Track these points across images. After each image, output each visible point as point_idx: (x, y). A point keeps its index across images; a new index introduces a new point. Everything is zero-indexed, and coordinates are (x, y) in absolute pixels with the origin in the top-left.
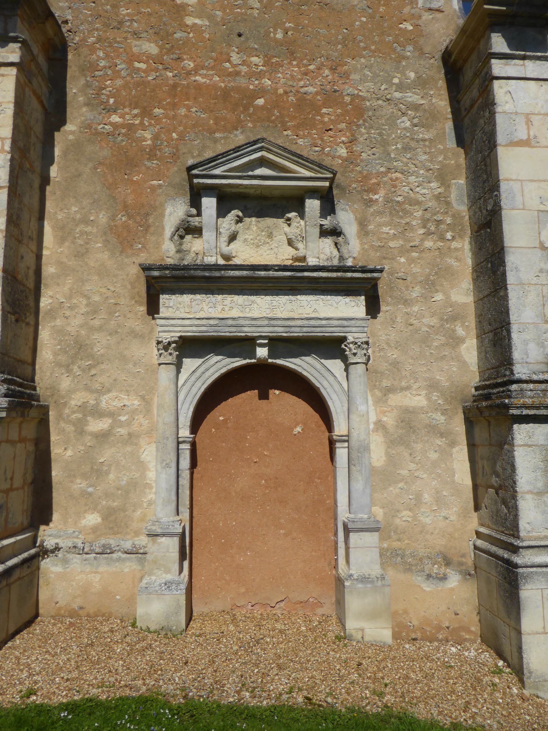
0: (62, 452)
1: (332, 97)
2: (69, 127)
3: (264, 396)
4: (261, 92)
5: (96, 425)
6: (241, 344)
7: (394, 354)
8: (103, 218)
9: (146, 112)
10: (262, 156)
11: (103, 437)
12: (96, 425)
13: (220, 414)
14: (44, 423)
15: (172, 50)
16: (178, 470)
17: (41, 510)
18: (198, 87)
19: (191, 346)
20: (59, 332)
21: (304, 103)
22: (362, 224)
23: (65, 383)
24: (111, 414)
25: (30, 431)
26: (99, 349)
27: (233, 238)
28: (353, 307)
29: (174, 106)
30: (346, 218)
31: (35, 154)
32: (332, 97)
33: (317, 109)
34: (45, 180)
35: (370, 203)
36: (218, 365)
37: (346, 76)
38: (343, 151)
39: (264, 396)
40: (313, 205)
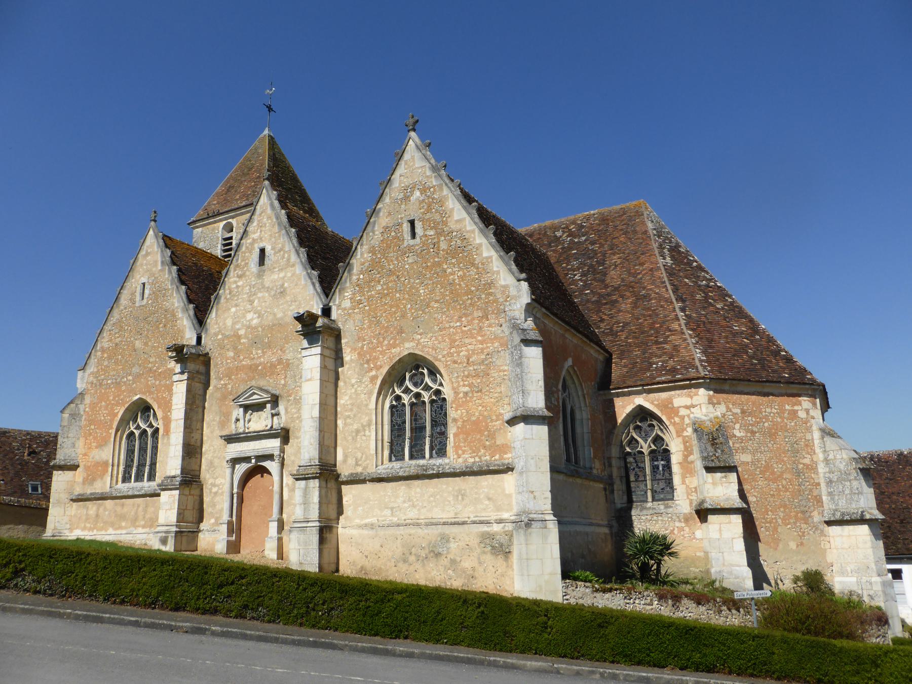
0: (206, 499)
1: (280, 361)
2: (211, 388)
3: (262, 476)
4: (260, 364)
5: (215, 490)
6: (247, 459)
7: (293, 458)
8: (217, 419)
9: (230, 379)
10: (140, 399)
11: (216, 493)
12: (215, 490)
13: (250, 484)
14: (202, 489)
15: (237, 352)
16: (455, 524)
17: (201, 519)
18: (244, 366)
19: (235, 461)
20: (206, 459)
21: (273, 366)
22: (286, 409)
23: (208, 476)
24: (218, 486)
25: (196, 492)
26: (216, 464)
27: (249, 421)
28: (275, 443)
29: (237, 374)
30: (281, 408)
31: (331, 387)
32: (280, 361)
33: (275, 367)
34: (204, 408)
35: (289, 401)
36: (242, 468)
37: (284, 352)
38: (283, 382)
39: (262, 476)
40: (269, 406)
